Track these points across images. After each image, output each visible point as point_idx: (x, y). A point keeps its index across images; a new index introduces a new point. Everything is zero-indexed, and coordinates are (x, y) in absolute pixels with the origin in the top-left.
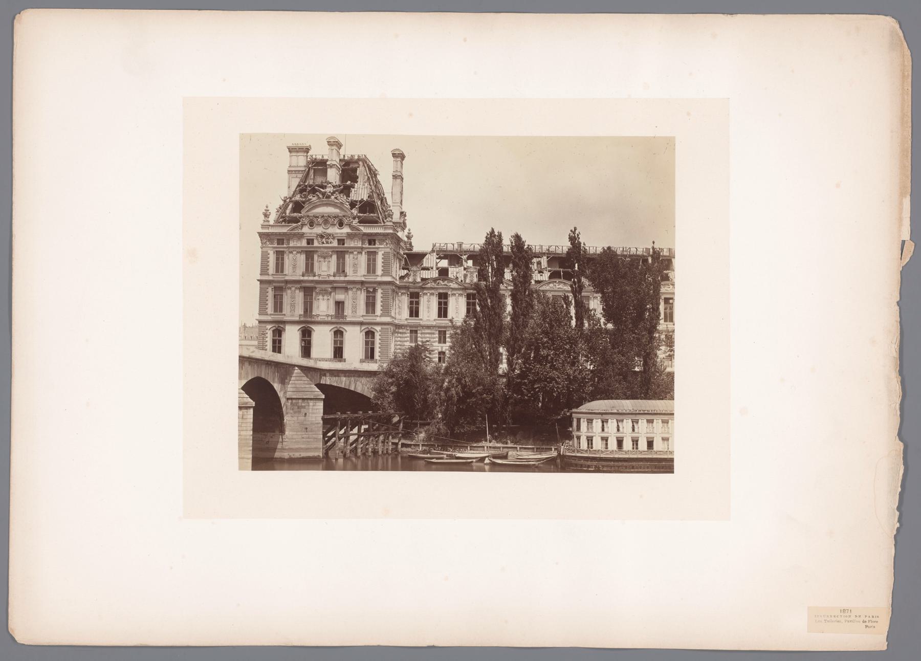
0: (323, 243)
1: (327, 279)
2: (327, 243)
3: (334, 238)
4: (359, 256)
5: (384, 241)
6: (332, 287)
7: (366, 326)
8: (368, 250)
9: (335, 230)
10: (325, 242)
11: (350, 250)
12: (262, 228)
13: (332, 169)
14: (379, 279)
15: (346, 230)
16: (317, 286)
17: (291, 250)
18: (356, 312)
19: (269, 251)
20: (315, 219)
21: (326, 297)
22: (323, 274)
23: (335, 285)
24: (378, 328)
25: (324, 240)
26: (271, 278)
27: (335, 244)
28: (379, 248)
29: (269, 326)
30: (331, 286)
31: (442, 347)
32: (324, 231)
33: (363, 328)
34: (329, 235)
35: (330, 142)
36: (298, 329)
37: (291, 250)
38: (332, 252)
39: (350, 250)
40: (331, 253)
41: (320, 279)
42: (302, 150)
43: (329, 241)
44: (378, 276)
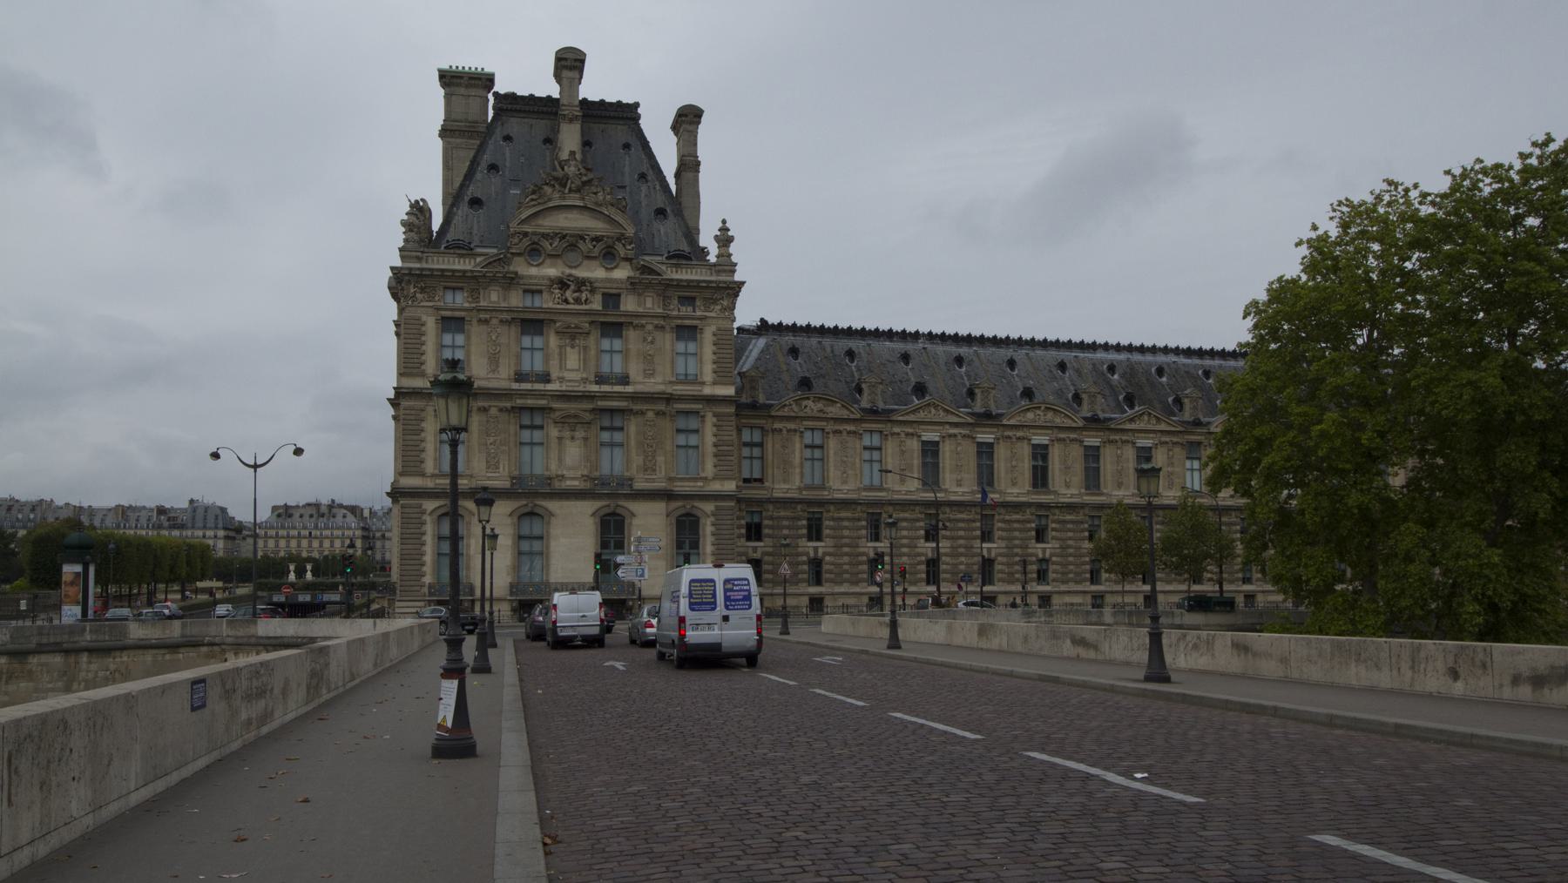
0: (566, 301)
1: (581, 389)
2: (578, 301)
3: (593, 291)
4: (658, 335)
5: (715, 302)
6: (594, 409)
7: (679, 504)
8: (679, 322)
10: (571, 300)
11: (636, 322)
12: (402, 257)
13: (572, 125)
14: (707, 391)
15: (622, 273)
16: (555, 405)
17: (483, 316)
18: (655, 470)
19: (424, 318)
20: (546, 244)
21: (580, 434)
23: (601, 404)
24: (709, 507)
25: (568, 294)
27: (596, 305)
28: (706, 317)
29: (430, 505)
30: (591, 406)
31: (1044, 550)
32: (568, 271)
33: (671, 508)
34: (581, 283)
35: (566, 59)
36: (510, 510)
37: (483, 316)
38: (592, 323)
39: (636, 322)
40: (587, 325)
41: (564, 388)
42: (477, 82)
43: (584, 297)
44: (703, 383)
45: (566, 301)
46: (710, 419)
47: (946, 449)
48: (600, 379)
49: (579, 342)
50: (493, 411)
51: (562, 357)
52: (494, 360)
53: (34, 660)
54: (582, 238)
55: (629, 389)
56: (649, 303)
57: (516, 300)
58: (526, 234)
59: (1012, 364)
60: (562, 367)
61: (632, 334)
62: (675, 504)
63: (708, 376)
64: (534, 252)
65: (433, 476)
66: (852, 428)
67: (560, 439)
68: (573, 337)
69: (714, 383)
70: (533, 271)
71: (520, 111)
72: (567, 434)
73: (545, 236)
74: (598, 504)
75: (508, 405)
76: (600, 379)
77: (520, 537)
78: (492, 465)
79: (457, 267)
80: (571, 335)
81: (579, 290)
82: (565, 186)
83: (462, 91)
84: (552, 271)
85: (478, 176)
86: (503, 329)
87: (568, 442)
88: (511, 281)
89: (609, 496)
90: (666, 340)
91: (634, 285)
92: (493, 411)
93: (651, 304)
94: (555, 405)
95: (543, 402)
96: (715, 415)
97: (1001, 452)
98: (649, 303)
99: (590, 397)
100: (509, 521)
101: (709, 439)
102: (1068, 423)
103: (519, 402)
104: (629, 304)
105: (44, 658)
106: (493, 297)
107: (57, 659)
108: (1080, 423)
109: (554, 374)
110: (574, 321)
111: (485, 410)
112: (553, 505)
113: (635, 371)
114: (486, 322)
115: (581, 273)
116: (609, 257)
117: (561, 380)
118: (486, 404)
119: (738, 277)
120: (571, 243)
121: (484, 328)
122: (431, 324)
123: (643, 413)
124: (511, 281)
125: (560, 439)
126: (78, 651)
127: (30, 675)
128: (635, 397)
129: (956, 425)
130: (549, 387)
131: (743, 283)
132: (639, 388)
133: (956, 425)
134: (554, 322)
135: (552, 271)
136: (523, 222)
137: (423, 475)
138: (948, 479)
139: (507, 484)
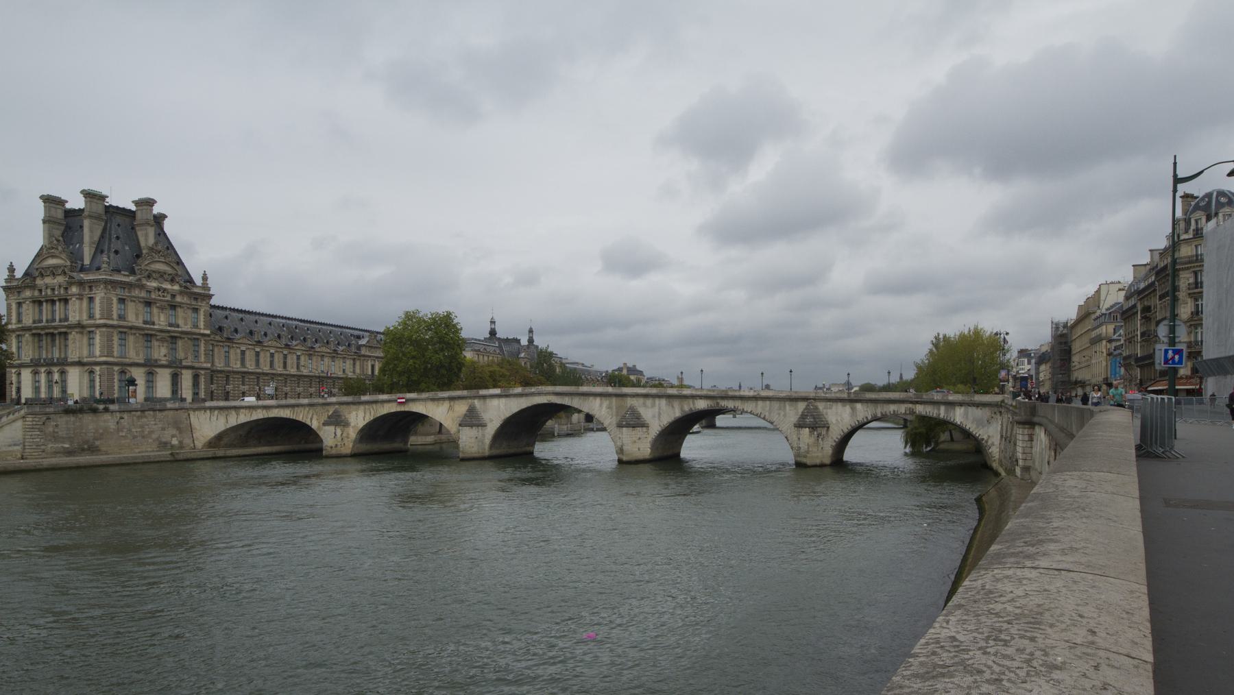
0: (159, 296)
2: (164, 296)
9: (167, 286)
14: (202, 331)
15: (176, 287)
16: (158, 334)
19: (113, 298)
20: (154, 275)
22: (162, 323)
23: (173, 334)
24: (203, 372)
25: (160, 293)
26: (115, 323)
27: (168, 298)
29: (116, 368)
34: (165, 290)
44: (201, 329)
45: (159, 296)
46: (203, 342)
47: (247, 353)
48: (171, 325)
49: (164, 311)
50: (137, 335)
51: (159, 318)
52: (137, 315)
53: (146, 413)
54: (165, 273)
55: (180, 329)
56: (185, 299)
57: (143, 294)
58: (147, 270)
59: (256, 322)
60: (159, 320)
61: (179, 310)
62: (194, 371)
63: (202, 327)
64: (149, 277)
65: (117, 357)
66: (221, 344)
67: (159, 346)
68: (162, 309)
69: (204, 329)
70: (148, 284)
71: (120, 214)
72: (161, 344)
73: (154, 271)
74: (171, 370)
75: (143, 333)
76: (171, 325)
77: (152, 382)
78: (138, 354)
79: (124, 280)
80: (162, 308)
81: (163, 292)
82: (159, 253)
83: (95, 201)
84: (154, 284)
85: (113, 240)
86: (139, 304)
87: (161, 347)
88: (142, 287)
89: (175, 367)
90: (189, 312)
91: (181, 293)
92: (137, 335)
93: (185, 300)
94: (158, 334)
95: (154, 332)
96: (205, 340)
97: (262, 355)
98: (185, 299)
99: (168, 332)
100: (144, 375)
101: (203, 349)
102: (279, 345)
103: (146, 332)
104: (179, 299)
105: (149, 412)
106: (136, 292)
107: (151, 413)
108: (283, 346)
109: (156, 322)
110: (164, 303)
111: (135, 334)
112: (158, 370)
113: (180, 322)
114: (134, 301)
115: (164, 286)
116: (172, 281)
117: (159, 324)
118: (135, 332)
119: (211, 292)
120: (162, 275)
121: (133, 303)
122: (115, 300)
123: (184, 338)
124: (142, 287)
125: (159, 346)
126: (156, 410)
127: (146, 417)
128: (182, 333)
129: (251, 345)
130: (155, 327)
131: (213, 295)
132: (184, 329)
133: (251, 345)
134: (156, 303)
135: (154, 284)
136: (146, 265)
137: (113, 357)
138: (248, 364)
139: (143, 362)
